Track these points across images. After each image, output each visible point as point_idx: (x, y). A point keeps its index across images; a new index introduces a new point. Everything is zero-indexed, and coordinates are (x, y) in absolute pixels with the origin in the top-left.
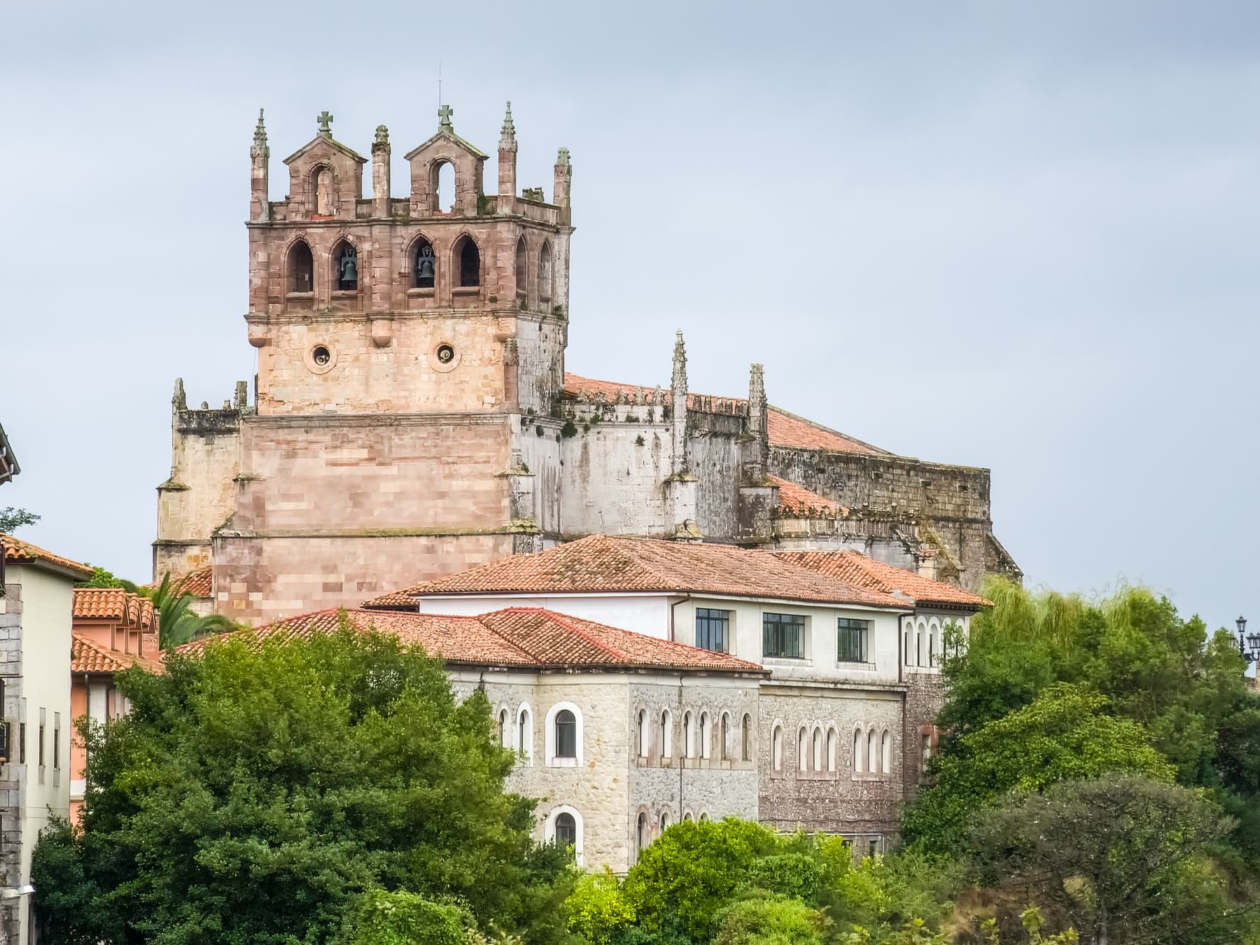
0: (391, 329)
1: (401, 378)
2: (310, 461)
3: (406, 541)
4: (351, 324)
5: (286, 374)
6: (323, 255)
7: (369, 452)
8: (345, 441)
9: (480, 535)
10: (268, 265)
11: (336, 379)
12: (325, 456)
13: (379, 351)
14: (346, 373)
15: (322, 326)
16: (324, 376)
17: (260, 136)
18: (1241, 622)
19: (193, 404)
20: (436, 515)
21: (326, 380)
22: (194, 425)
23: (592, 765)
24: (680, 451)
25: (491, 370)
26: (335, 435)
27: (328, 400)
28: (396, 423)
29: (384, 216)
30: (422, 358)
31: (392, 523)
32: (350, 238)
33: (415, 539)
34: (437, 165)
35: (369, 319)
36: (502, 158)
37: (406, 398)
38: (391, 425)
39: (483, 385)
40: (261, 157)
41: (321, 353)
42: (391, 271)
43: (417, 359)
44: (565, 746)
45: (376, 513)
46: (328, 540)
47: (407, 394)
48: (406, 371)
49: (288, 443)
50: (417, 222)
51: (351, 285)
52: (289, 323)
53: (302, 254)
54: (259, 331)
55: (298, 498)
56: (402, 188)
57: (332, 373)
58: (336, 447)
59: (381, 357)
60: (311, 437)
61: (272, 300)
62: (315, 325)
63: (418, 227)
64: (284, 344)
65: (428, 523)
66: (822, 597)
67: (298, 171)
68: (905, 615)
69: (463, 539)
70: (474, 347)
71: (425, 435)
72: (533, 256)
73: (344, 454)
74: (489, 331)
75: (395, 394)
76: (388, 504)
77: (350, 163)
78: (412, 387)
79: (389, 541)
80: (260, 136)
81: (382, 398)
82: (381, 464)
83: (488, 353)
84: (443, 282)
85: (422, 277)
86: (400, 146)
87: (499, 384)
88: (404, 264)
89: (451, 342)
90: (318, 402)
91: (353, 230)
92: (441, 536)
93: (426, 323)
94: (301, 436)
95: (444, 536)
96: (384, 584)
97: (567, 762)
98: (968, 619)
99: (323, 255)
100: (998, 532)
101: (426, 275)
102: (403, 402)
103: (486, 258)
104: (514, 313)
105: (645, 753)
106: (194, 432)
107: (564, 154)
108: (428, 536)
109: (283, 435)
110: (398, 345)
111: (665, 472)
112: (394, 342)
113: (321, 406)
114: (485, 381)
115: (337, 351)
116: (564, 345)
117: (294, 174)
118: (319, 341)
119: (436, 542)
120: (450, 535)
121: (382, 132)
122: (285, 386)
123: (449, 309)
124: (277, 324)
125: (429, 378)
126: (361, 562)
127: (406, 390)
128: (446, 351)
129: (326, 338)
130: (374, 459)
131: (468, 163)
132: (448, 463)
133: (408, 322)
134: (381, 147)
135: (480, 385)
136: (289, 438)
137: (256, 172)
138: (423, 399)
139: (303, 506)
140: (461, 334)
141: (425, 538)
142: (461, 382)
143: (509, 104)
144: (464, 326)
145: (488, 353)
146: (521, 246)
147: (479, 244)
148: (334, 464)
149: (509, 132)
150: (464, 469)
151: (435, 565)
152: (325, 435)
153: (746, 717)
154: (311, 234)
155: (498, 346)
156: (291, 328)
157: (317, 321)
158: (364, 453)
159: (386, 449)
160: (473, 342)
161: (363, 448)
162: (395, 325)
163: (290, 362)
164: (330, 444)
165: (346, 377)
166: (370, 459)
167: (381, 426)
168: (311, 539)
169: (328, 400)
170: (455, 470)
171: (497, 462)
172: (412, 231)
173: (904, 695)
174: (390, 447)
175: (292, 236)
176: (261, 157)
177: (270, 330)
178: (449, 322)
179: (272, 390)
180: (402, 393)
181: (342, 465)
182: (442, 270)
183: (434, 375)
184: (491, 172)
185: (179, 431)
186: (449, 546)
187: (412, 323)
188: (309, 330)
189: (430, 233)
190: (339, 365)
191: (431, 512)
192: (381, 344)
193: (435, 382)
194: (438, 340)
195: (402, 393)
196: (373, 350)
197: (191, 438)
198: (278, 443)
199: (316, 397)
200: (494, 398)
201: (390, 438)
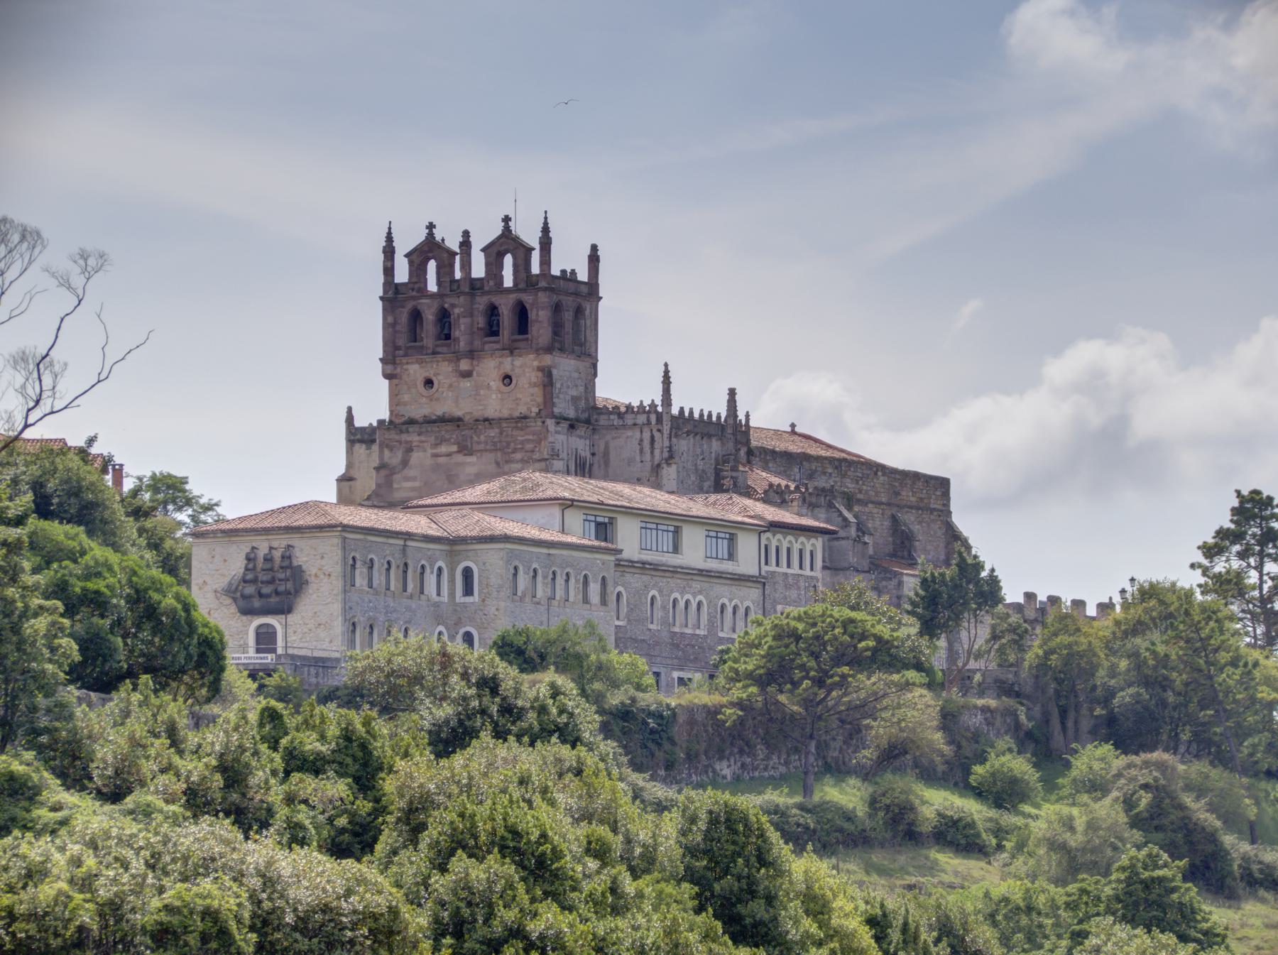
0: (472, 364)
1: (478, 398)
5: (406, 397)
6: (429, 316)
11: (438, 399)
12: (430, 451)
15: (429, 365)
16: (431, 399)
18: (1132, 580)
19: (358, 423)
21: (431, 400)
22: (359, 437)
23: (484, 600)
24: (667, 443)
29: (467, 290)
30: (492, 383)
32: (446, 306)
34: (501, 255)
36: (542, 249)
40: (389, 252)
41: (429, 383)
42: (472, 325)
44: (468, 590)
48: (482, 392)
49: (407, 442)
50: (489, 293)
51: (448, 337)
52: (407, 363)
53: (416, 316)
54: (390, 369)
55: (414, 479)
56: (479, 269)
59: (466, 384)
60: (423, 438)
61: (397, 348)
64: (405, 377)
66: (691, 514)
68: (765, 531)
72: (568, 316)
73: (443, 449)
77: (445, 255)
82: (465, 455)
83: (534, 379)
85: (492, 330)
86: (478, 244)
87: (540, 400)
88: (481, 321)
89: (510, 373)
94: (415, 438)
97: (469, 599)
98: (820, 540)
99: (429, 316)
101: (495, 328)
103: (532, 315)
104: (549, 350)
105: (519, 593)
106: (361, 441)
107: (594, 248)
111: (657, 459)
112: (475, 373)
116: (595, 375)
117: (411, 263)
118: (427, 374)
121: (466, 234)
123: (511, 350)
128: (507, 379)
131: (521, 253)
134: (466, 244)
136: (409, 439)
139: (417, 484)
143: (546, 212)
144: (518, 362)
146: (557, 308)
147: (528, 306)
148: (435, 456)
149: (546, 230)
150: (518, 456)
153: (604, 579)
155: (540, 374)
156: (409, 367)
158: (455, 448)
159: (469, 444)
166: (459, 452)
171: (539, 451)
173: (764, 584)
176: (389, 252)
177: (395, 368)
178: (509, 359)
179: (398, 408)
180: (481, 407)
184: (536, 258)
189: (497, 300)
192: (467, 375)
195: (481, 407)
197: (357, 446)
198: (400, 442)
201: (472, 438)
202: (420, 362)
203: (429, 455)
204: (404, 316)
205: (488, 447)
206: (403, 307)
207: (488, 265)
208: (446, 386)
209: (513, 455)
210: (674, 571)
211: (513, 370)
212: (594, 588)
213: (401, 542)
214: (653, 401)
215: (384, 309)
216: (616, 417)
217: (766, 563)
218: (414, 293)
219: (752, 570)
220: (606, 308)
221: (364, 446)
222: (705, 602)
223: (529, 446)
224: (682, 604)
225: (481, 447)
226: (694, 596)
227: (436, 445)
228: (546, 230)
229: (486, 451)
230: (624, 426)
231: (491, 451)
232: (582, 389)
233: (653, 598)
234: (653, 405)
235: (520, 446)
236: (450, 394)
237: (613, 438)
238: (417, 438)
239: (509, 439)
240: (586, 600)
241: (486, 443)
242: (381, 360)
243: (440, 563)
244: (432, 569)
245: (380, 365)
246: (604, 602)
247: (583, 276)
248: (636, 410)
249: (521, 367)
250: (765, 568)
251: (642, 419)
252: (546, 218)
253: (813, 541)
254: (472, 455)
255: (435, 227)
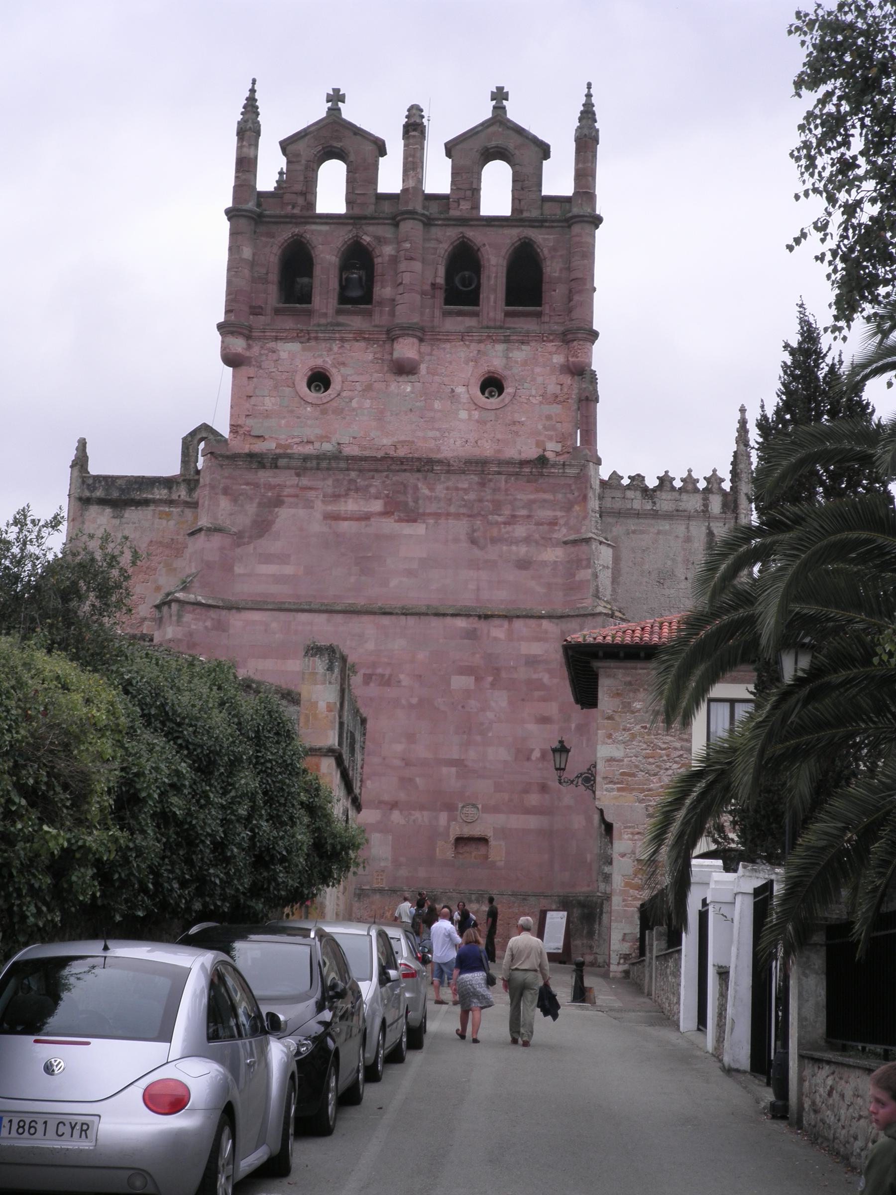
0: (419, 352)
2: (301, 512)
3: (435, 622)
4: (362, 344)
7: (386, 504)
8: (353, 489)
9: (541, 617)
10: (253, 264)
11: (339, 412)
13: (401, 379)
14: (354, 404)
15: (323, 345)
17: (251, 107)
19: (95, 468)
20: (478, 589)
21: (324, 412)
22: (99, 493)
25: (556, 409)
26: (338, 480)
27: (327, 437)
28: (426, 468)
30: (460, 390)
31: (417, 597)
32: (367, 239)
33: (449, 621)
35: (391, 336)
37: (435, 439)
38: (419, 471)
39: (544, 427)
43: (453, 391)
45: (393, 583)
46: (323, 617)
47: (438, 434)
48: (437, 405)
49: (271, 487)
52: (276, 339)
54: (238, 345)
55: (282, 559)
57: (334, 404)
58: (339, 496)
60: (305, 481)
61: (256, 311)
62: (313, 343)
63: (461, 229)
64: (269, 364)
65: (467, 599)
67: (298, 155)
69: (518, 624)
70: (534, 380)
71: (466, 486)
73: (351, 506)
74: (555, 361)
75: (419, 434)
76: (410, 573)
78: (445, 426)
79: (411, 621)
80: (251, 107)
81: (403, 438)
82: (400, 520)
83: (552, 388)
84: (492, 297)
90: (312, 438)
91: (371, 229)
92: (487, 617)
93: (468, 346)
95: (492, 616)
96: (402, 677)
102: (432, 444)
106: (102, 502)
108: (468, 616)
109: (265, 476)
110: (428, 373)
112: (423, 368)
113: (317, 445)
114: (548, 423)
115: (342, 376)
118: (319, 362)
119: (482, 625)
120: (499, 616)
122: (267, 417)
124: (259, 339)
125: (470, 416)
126: (370, 646)
127: (438, 430)
129: (327, 359)
130: (393, 514)
132: (497, 523)
133: (443, 346)
135: (540, 427)
136: (273, 481)
137: (245, 150)
138: (458, 443)
139: (289, 570)
140: (516, 362)
141: (464, 619)
142: (514, 423)
143: (589, 86)
144: (520, 354)
145: (552, 388)
150: (520, 531)
151: (478, 656)
152: (324, 479)
154: (313, 232)
155: (567, 380)
157: (316, 339)
158: (377, 506)
160: (533, 371)
161: (377, 498)
162: (425, 348)
163: (276, 387)
164: (330, 491)
165: (354, 410)
166: (386, 513)
167: (405, 470)
168: (300, 614)
169: (325, 438)
170: (508, 532)
172: (452, 234)
174: (416, 500)
175: (285, 234)
177: (249, 347)
178: (500, 347)
179: (250, 422)
180: (431, 434)
181: (345, 519)
182: (492, 282)
183: (476, 413)
185: (80, 499)
186: (498, 631)
187: (448, 346)
188: (304, 349)
189: (475, 235)
190: (344, 394)
191: (472, 586)
192: (404, 369)
193: (478, 421)
194: (483, 369)
195: (431, 434)
196: (390, 377)
197: (94, 510)
199: (310, 432)
200: (560, 445)
201: (416, 488)
202: (304, 337)
203: (319, 516)
204: (272, 255)
205: (452, 510)
206: (271, 235)
207: (456, 173)
208: (358, 386)
209: (509, 528)
211: (507, 367)
214: (715, 471)
215: (234, 234)
216: (638, 494)
218: (296, 211)
221: (108, 511)
223: (546, 514)
225: (432, 508)
227: (336, 497)
228: (588, 114)
229: (448, 515)
230: (655, 515)
231: (457, 516)
234: (714, 480)
235: (524, 512)
236: (367, 403)
237: (628, 533)
238: (295, 480)
239: (500, 497)
241: (450, 501)
242: (220, 327)
245: (218, 338)
248: (678, 484)
249: (525, 363)
251: (693, 503)
252: (589, 96)
254: (415, 521)
255: (342, 99)
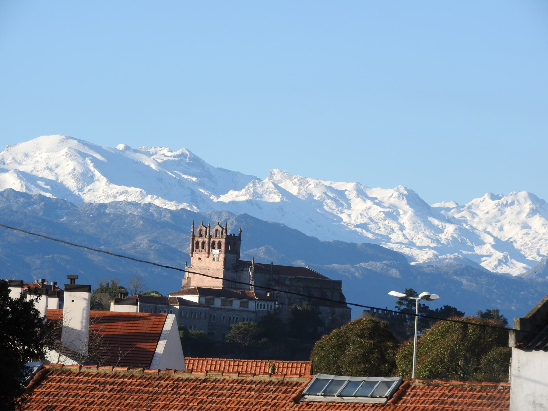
55: (195, 281)
100: (342, 291)
139: (196, 282)
153: (206, 313)
173: (256, 313)
210: (230, 310)
212: (203, 315)
213: (155, 305)
217: (258, 308)
219: (253, 309)
220: (242, 243)
222: (239, 317)
224: (232, 317)
226: (236, 316)
232: (235, 261)
233: (224, 316)
240: (200, 318)
243: (165, 309)
244: (163, 311)
246: (205, 318)
247: (237, 235)
250: (257, 309)
253: (272, 303)
